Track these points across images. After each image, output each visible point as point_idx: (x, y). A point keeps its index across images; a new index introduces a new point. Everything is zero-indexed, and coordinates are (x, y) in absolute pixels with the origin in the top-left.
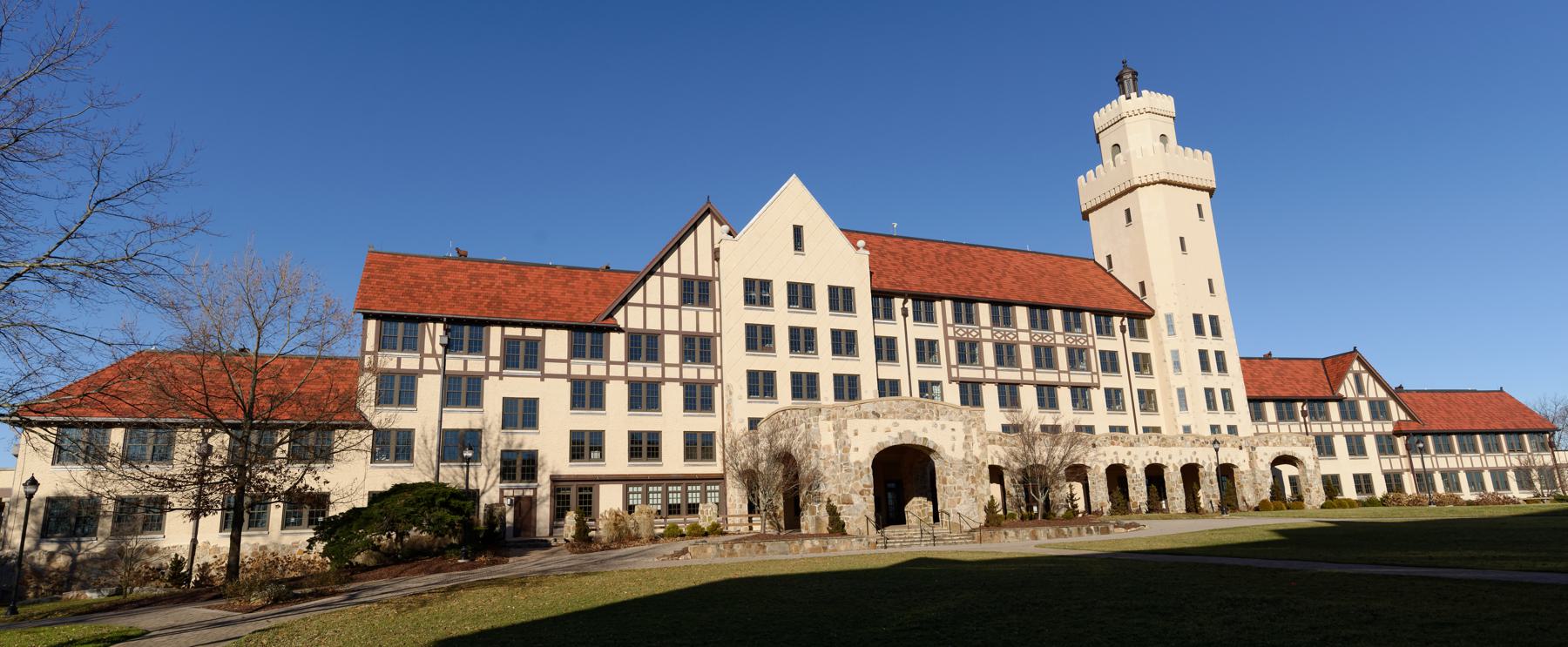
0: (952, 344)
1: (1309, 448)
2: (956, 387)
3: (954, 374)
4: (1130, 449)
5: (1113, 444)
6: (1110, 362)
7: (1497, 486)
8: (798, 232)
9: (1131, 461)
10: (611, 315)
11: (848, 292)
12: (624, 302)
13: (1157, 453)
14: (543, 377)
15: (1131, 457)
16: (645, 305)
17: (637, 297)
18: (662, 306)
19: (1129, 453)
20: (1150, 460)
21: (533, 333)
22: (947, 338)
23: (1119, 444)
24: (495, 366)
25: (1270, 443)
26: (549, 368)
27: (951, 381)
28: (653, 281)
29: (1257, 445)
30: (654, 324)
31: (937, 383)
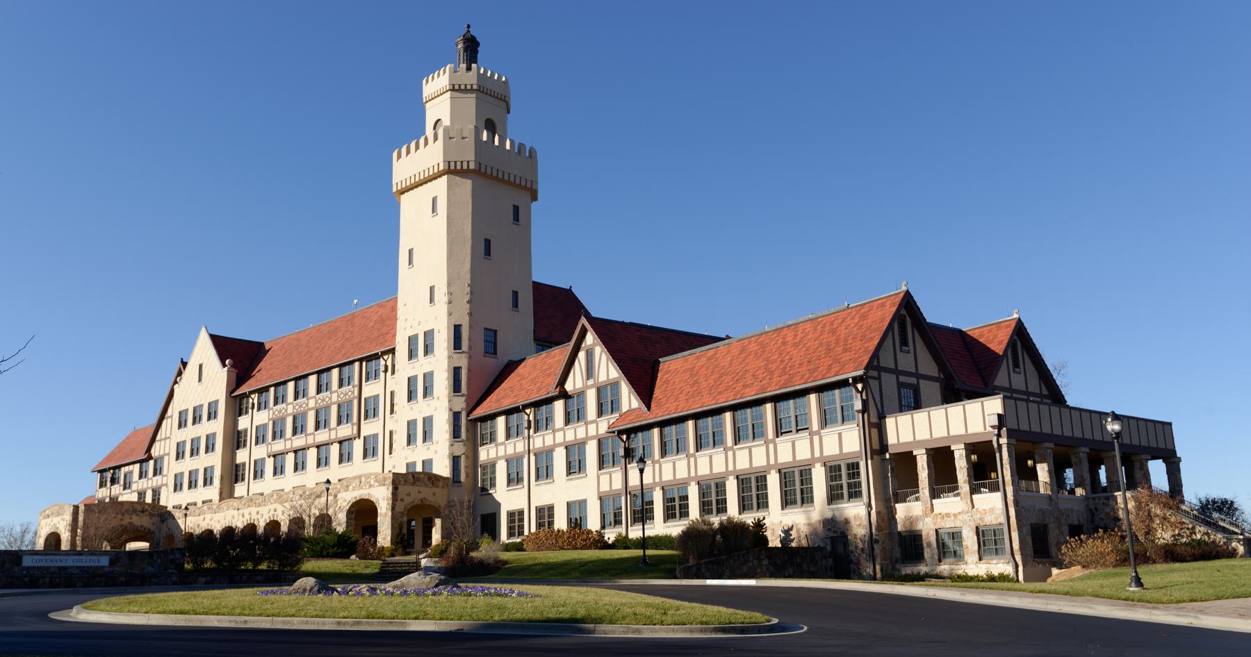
0: (271, 423)
1: (386, 487)
2: (272, 459)
3: (269, 451)
4: (259, 509)
5: (249, 506)
6: (370, 410)
7: (744, 506)
8: (201, 366)
9: (258, 519)
10: (149, 450)
11: (216, 402)
12: (153, 440)
13: (275, 510)
14: (133, 492)
15: (259, 516)
16: (161, 440)
17: (158, 438)
18: (165, 439)
19: (258, 513)
20: (270, 517)
21: (131, 467)
22: (269, 420)
23: (252, 506)
24: (122, 488)
25: (351, 488)
26: (134, 487)
27: (269, 457)
28: (164, 422)
29: (339, 492)
30: (162, 453)
31: (264, 458)
